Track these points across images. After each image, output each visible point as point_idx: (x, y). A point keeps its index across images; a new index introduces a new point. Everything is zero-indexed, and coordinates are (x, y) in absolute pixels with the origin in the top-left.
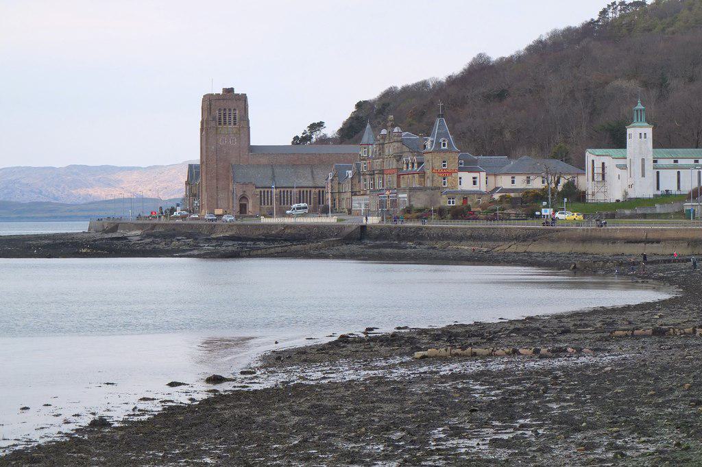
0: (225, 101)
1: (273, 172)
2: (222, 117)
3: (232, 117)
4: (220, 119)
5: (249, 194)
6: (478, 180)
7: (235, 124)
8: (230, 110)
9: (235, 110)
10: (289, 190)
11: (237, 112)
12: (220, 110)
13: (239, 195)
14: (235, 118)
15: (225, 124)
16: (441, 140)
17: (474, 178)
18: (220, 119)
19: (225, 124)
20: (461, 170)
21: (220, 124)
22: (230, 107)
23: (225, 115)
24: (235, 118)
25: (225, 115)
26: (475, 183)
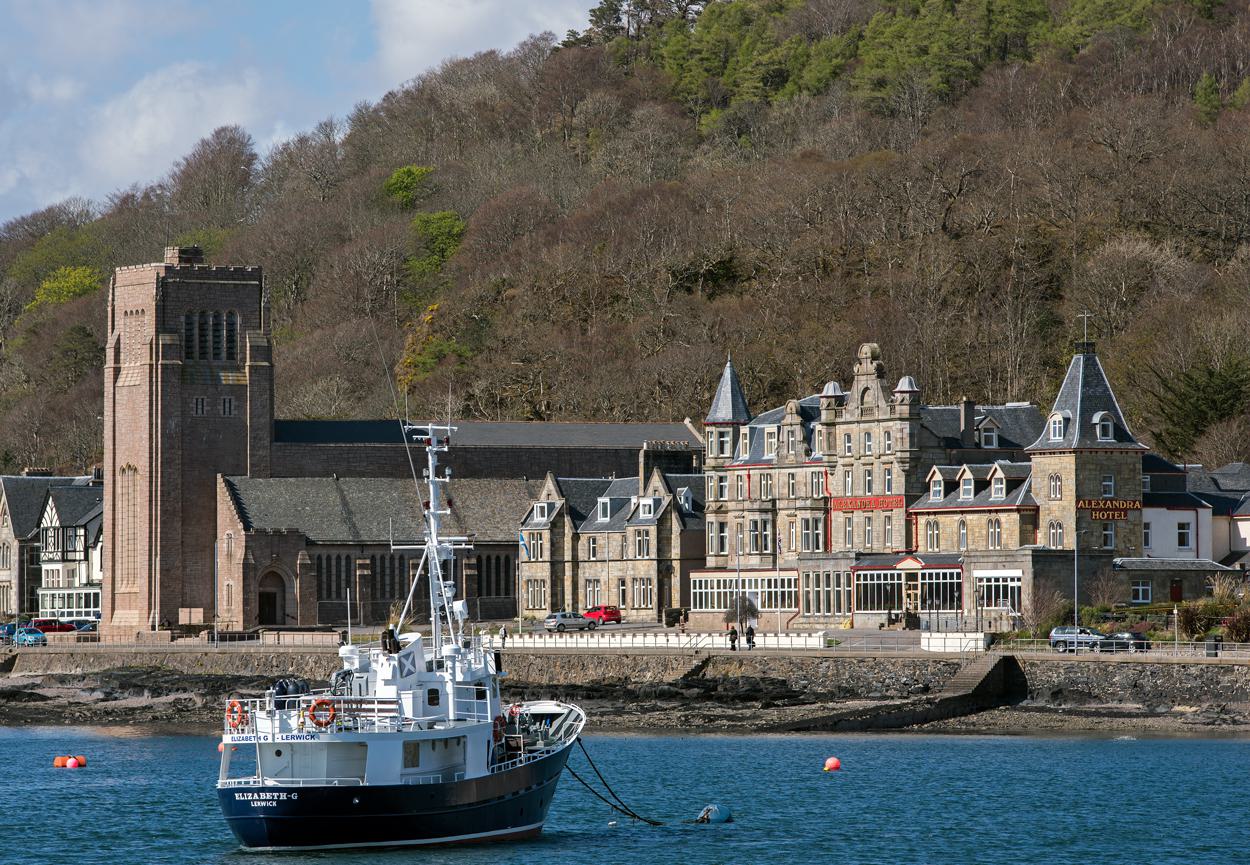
1: (343, 498)
6: (1191, 533)
9: (231, 314)
16: (1096, 418)
17: (1182, 526)
18: (189, 339)
19: (203, 354)
20: (1150, 501)
26: (1183, 540)
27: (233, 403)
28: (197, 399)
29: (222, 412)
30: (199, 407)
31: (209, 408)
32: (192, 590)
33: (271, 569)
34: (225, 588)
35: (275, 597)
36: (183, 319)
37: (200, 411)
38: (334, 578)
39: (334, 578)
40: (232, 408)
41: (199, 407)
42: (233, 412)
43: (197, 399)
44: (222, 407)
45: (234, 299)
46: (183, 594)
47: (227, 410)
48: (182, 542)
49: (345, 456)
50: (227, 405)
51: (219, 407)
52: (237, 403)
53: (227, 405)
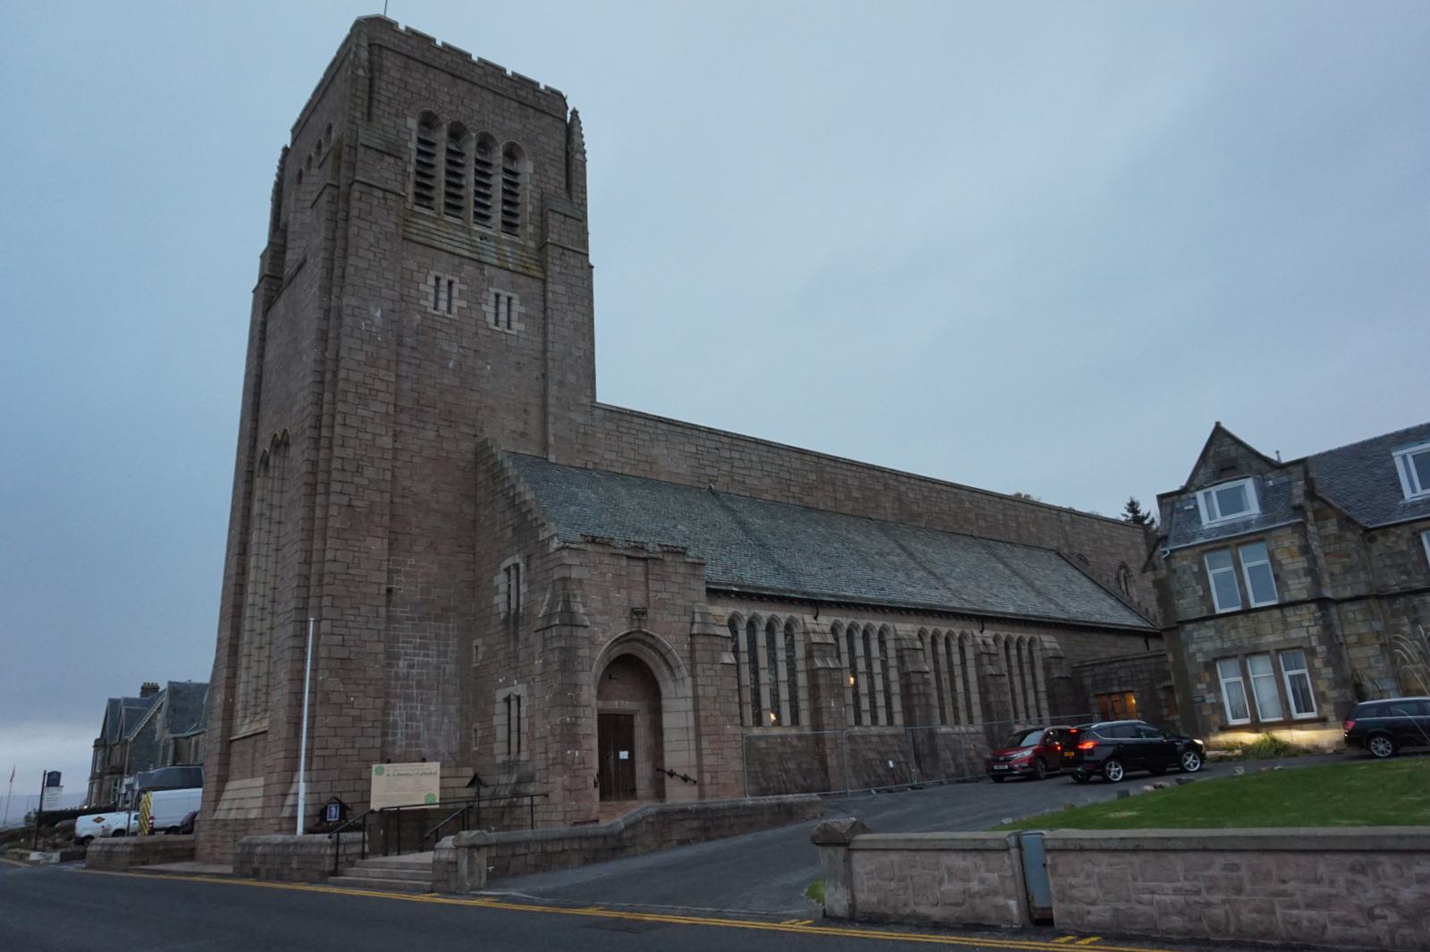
0: (462, 87)
2: (441, 159)
3: (497, 181)
4: (424, 170)
5: (668, 630)
9: (511, 153)
11: (526, 167)
12: (428, 121)
13: (605, 640)
15: (454, 207)
18: (424, 170)
19: (454, 207)
21: (423, 196)
22: (489, 130)
23: (454, 159)
25: (454, 159)
27: (517, 308)
29: (491, 319)
30: (443, 296)
31: (464, 304)
32: (410, 718)
34: (500, 708)
35: (631, 727)
36: (413, 123)
37: (443, 305)
40: (514, 316)
41: (443, 296)
42: (515, 325)
43: (437, 279)
44: (493, 310)
46: (386, 728)
47: (503, 317)
48: (389, 591)
49: (726, 454)
50: (503, 308)
51: (484, 307)
52: (523, 310)
53: (503, 308)
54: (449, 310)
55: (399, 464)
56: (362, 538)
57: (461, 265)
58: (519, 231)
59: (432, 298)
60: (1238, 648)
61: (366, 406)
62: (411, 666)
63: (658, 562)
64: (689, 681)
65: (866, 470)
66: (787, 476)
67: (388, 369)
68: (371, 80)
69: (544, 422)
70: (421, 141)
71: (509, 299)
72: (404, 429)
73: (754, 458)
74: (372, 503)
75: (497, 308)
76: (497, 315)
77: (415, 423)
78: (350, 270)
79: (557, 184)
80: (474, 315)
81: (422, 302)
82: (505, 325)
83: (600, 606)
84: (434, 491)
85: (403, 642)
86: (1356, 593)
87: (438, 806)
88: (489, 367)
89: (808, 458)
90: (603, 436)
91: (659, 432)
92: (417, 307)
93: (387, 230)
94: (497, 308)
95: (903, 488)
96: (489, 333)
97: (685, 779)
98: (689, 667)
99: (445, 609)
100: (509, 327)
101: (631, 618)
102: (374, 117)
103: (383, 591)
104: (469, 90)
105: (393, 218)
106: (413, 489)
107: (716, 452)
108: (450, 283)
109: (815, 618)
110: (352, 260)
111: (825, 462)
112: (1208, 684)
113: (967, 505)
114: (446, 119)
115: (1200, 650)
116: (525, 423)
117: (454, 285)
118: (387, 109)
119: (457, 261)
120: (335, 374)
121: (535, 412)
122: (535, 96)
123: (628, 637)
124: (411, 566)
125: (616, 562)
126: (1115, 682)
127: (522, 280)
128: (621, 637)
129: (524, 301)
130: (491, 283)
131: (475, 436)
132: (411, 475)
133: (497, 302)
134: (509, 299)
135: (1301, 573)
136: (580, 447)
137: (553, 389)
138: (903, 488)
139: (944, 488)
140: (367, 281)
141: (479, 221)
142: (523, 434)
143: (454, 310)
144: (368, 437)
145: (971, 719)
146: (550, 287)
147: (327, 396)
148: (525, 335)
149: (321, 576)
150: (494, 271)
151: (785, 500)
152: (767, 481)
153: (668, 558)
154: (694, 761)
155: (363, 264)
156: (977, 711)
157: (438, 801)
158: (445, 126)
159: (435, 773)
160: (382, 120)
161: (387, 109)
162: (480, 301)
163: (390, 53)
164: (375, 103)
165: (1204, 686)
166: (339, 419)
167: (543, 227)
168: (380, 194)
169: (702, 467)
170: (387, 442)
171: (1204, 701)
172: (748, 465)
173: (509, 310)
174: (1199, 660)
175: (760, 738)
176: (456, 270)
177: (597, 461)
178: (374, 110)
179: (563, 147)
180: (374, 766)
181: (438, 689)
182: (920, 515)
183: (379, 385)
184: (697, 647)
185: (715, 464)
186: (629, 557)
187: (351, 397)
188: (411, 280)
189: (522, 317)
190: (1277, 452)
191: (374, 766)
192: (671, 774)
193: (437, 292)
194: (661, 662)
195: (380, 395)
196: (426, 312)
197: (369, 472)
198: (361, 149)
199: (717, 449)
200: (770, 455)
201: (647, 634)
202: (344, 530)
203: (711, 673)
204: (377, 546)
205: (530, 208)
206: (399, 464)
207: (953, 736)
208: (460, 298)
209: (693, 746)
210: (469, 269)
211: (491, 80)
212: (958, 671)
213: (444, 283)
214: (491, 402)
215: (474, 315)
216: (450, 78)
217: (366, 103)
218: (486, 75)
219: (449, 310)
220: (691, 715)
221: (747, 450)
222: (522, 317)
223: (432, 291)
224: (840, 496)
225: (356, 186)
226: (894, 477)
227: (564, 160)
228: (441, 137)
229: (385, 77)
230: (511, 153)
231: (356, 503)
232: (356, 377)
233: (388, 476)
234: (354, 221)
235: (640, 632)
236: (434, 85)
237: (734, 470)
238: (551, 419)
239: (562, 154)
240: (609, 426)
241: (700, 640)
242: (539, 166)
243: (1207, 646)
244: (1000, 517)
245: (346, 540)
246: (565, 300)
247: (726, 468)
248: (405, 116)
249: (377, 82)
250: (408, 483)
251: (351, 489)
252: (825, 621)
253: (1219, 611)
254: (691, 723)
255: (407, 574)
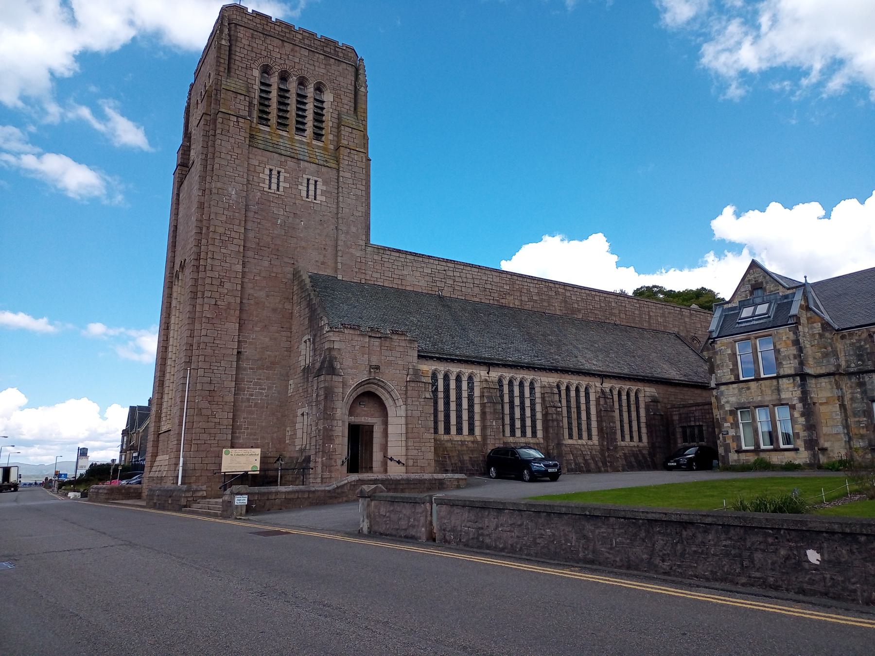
2: (274, 95)
3: (310, 107)
4: (264, 102)
7: (318, 136)
8: (302, 82)
9: (319, 88)
10: (528, 376)
11: (328, 97)
12: (266, 70)
13: (353, 383)
14: (319, 117)
15: (282, 124)
18: (264, 102)
19: (282, 124)
21: (264, 119)
23: (283, 94)
24: (319, 117)
28: (271, 170)
29: (304, 194)
30: (274, 180)
31: (287, 185)
33: (367, 388)
36: (256, 73)
37: (274, 186)
38: (453, 406)
39: (453, 406)
40: (319, 192)
41: (274, 180)
42: (318, 197)
43: (271, 170)
44: (306, 189)
45: (323, 71)
47: (312, 193)
48: (239, 353)
50: (312, 187)
51: (300, 187)
52: (324, 188)
53: (312, 187)
54: (278, 188)
55: (246, 280)
56: (223, 323)
57: (286, 161)
58: (323, 139)
59: (267, 182)
60: (749, 403)
61: (226, 247)
62: (252, 395)
63: (388, 340)
64: (403, 407)
65: (543, 283)
66: (489, 286)
67: (239, 225)
68: (230, 47)
69: (336, 256)
70: (262, 84)
71: (316, 182)
72: (250, 260)
73: (469, 276)
74: (229, 303)
75: (308, 187)
76: (308, 191)
77: (256, 256)
78: (216, 166)
79: (348, 107)
80: (294, 191)
81: (261, 185)
82: (313, 197)
83: (351, 364)
84: (268, 296)
85: (247, 382)
86: (828, 371)
87: (258, 472)
88: (302, 223)
89: (504, 275)
90: (372, 263)
91: (408, 260)
92: (258, 188)
93: (239, 141)
94: (308, 187)
95: (568, 294)
96: (302, 203)
97: (399, 462)
98: (404, 400)
99: (273, 363)
100: (315, 199)
101: (370, 371)
102: (233, 70)
103: (235, 353)
104: (292, 50)
105: (242, 134)
106: (255, 295)
107: (445, 272)
108: (279, 173)
109: (488, 373)
110: (217, 160)
111: (515, 278)
112: (731, 424)
113: (613, 304)
114: (276, 70)
115: (728, 402)
116: (324, 256)
117: (281, 174)
118: (240, 65)
119: (283, 159)
120: (208, 228)
121: (330, 250)
122: (335, 50)
123: (368, 381)
124: (253, 339)
125: (362, 339)
126: (693, 419)
127: (324, 169)
128: (362, 382)
129: (325, 183)
130: (304, 172)
131: (293, 264)
132: (254, 287)
133: (308, 184)
134: (316, 182)
135: (792, 357)
136: (357, 270)
137: (342, 237)
138: (568, 294)
139: (597, 293)
140: (227, 173)
141: (299, 133)
142: (323, 263)
143: (281, 189)
144: (228, 265)
145: (590, 437)
146: (341, 173)
147: (204, 241)
148: (326, 204)
149: (199, 344)
150: (306, 164)
151: (488, 302)
152: (476, 290)
153: (395, 337)
154: (404, 452)
155: (224, 163)
156: (595, 432)
157: (259, 469)
158: (277, 74)
159: (258, 455)
160: (237, 72)
161: (240, 65)
162: (297, 183)
163: (242, 28)
164: (233, 61)
165: (728, 424)
166: (210, 255)
167: (338, 135)
168: (235, 119)
169: (435, 282)
170: (239, 268)
171: (728, 434)
172: (465, 280)
173: (315, 189)
174: (726, 409)
175: (447, 441)
176: (281, 164)
177: (368, 278)
178: (232, 65)
179: (353, 84)
180: (224, 450)
181: (267, 407)
182: (579, 311)
183: (233, 235)
184: (409, 388)
185: (443, 280)
186: (370, 336)
187: (217, 242)
188: (255, 171)
189: (323, 193)
190: (805, 277)
191: (224, 450)
192: (391, 459)
193: (270, 177)
194: (388, 396)
195: (235, 240)
196: (264, 191)
197: (227, 285)
198: (223, 91)
199: (445, 271)
200: (479, 274)
201: (379, 380)
202: (213, 318)
203: (418, 403)
204: (233, 327)
205: (330, 124)
206: (246, 280)
207: (577, 446)
208: (284, 182)
209: (404, 444)
210: (291, 163)
211: (306, 42)
212: (583, 407)
213: (274, 173)
214: (303, 244)
215: (294, 191)
216: (281, 42)
217: (227, 62)
218: (303, 39)
219: (278, 188)
220: (404, 426)
221: (464, 271)
222: (323, 193)
223: (268, 178)
224: (525, 298)
225: (220, 115)
226: (563, 287)
227: (353, 92)
228: (274, 80)
229: (239, 44)
230: (319, 88)
231: (219, 303)
232: (221, 230)
233: (239, 287)
234: (218, 136)
235: (374, 379)
236: (270, 47)
237: (455, 283)
238: (340, 254)
239: (352, 88)
240: (376, 257)
241: (412, 384)
242: (337, 96)
243: (733, 399)
244: (637, 312)
245: (213, 324)
246: (351, 181)
247: (451, 282)
248: (251, 69)
249: (233, 48)
250: (251, 291)
251: (217, 295)
252: (495, 374)
253: (742, 379)
254: (404, 431)
255: (251, 343)
